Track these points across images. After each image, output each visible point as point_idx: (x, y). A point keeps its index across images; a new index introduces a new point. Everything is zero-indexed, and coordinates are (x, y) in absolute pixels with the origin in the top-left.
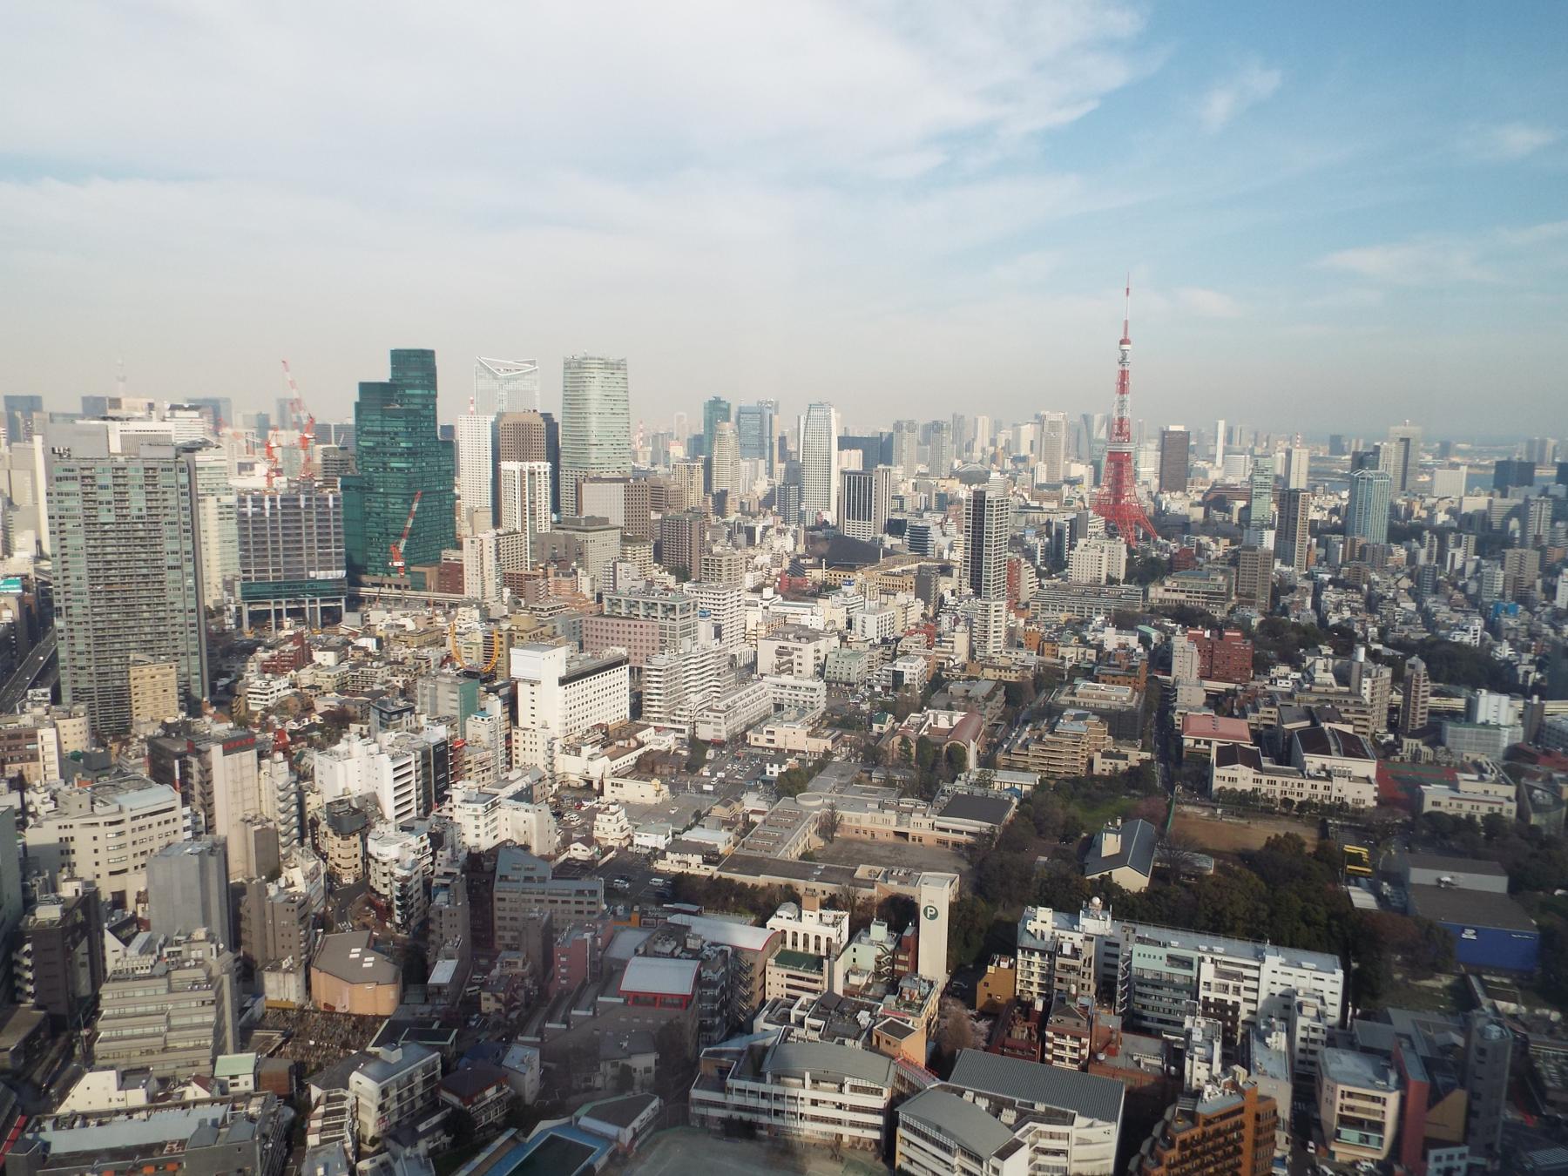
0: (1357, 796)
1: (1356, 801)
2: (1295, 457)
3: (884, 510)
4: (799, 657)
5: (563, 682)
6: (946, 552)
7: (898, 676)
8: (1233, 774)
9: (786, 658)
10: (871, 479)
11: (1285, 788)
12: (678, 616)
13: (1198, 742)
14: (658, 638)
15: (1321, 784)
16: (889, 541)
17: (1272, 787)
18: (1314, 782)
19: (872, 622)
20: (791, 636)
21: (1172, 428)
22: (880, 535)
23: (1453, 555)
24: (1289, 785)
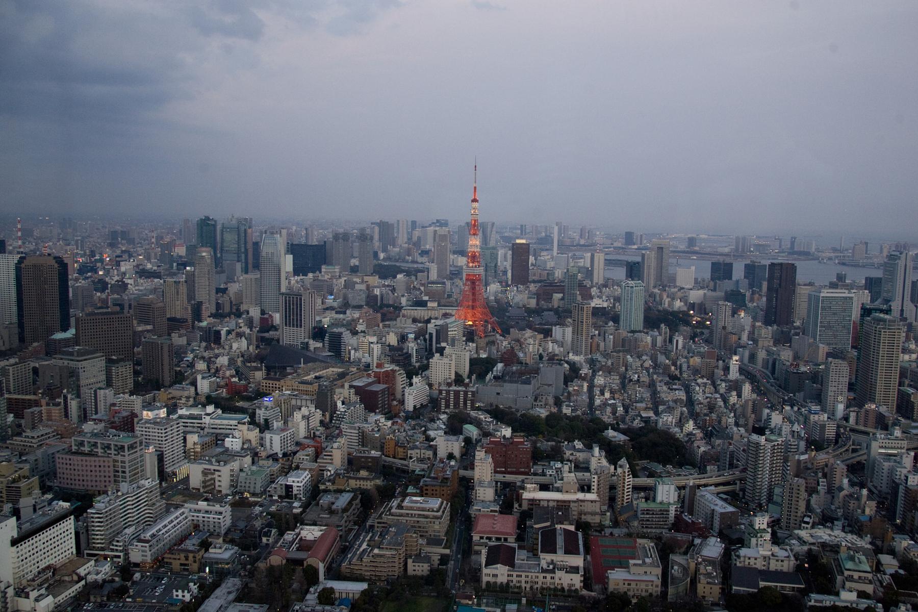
0: (570, 582)
1: (571, 585)
2: (596, 259)
3: (309, 322)
4: (219, 476)
5: (14, 542)
6: (353, 352)
7: (289, 488)
8: (495, 572)
9: (210, 477)
10: (301, 299)
11: (527, 579)
12: (127, 453)
13: (482, 538)
14: (112, 474)
15: (549, 576)
16: (314, 345)
17: (518, 579)
18: (544, 575)
19: (277, 439)
20: (214, 460)
21: (518, 241)
22: (306, 340)
23: (677, 341)
24: (530, 577)
